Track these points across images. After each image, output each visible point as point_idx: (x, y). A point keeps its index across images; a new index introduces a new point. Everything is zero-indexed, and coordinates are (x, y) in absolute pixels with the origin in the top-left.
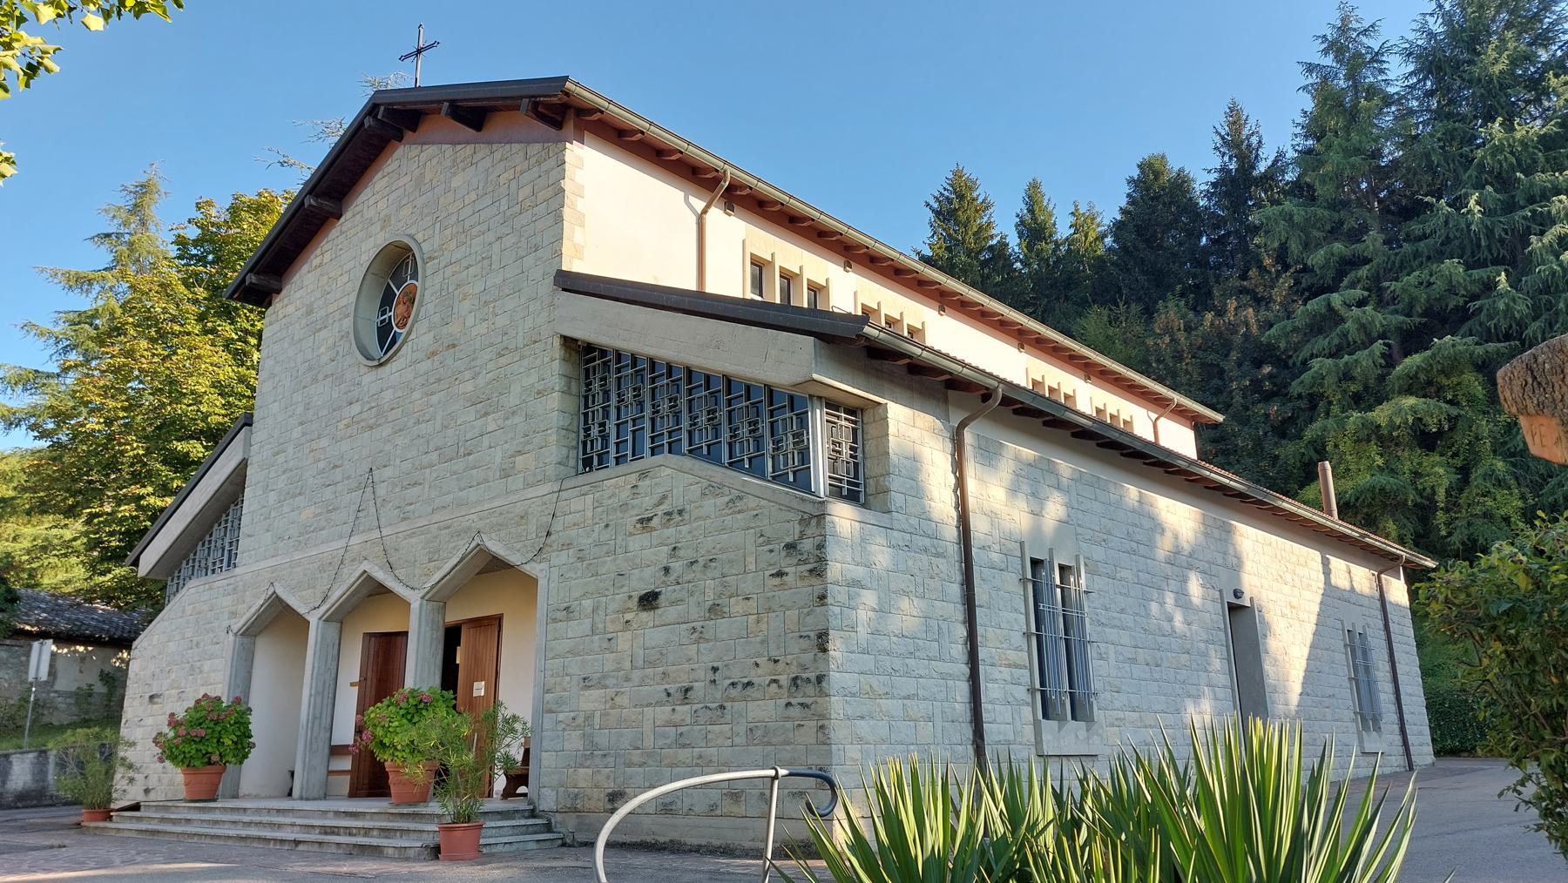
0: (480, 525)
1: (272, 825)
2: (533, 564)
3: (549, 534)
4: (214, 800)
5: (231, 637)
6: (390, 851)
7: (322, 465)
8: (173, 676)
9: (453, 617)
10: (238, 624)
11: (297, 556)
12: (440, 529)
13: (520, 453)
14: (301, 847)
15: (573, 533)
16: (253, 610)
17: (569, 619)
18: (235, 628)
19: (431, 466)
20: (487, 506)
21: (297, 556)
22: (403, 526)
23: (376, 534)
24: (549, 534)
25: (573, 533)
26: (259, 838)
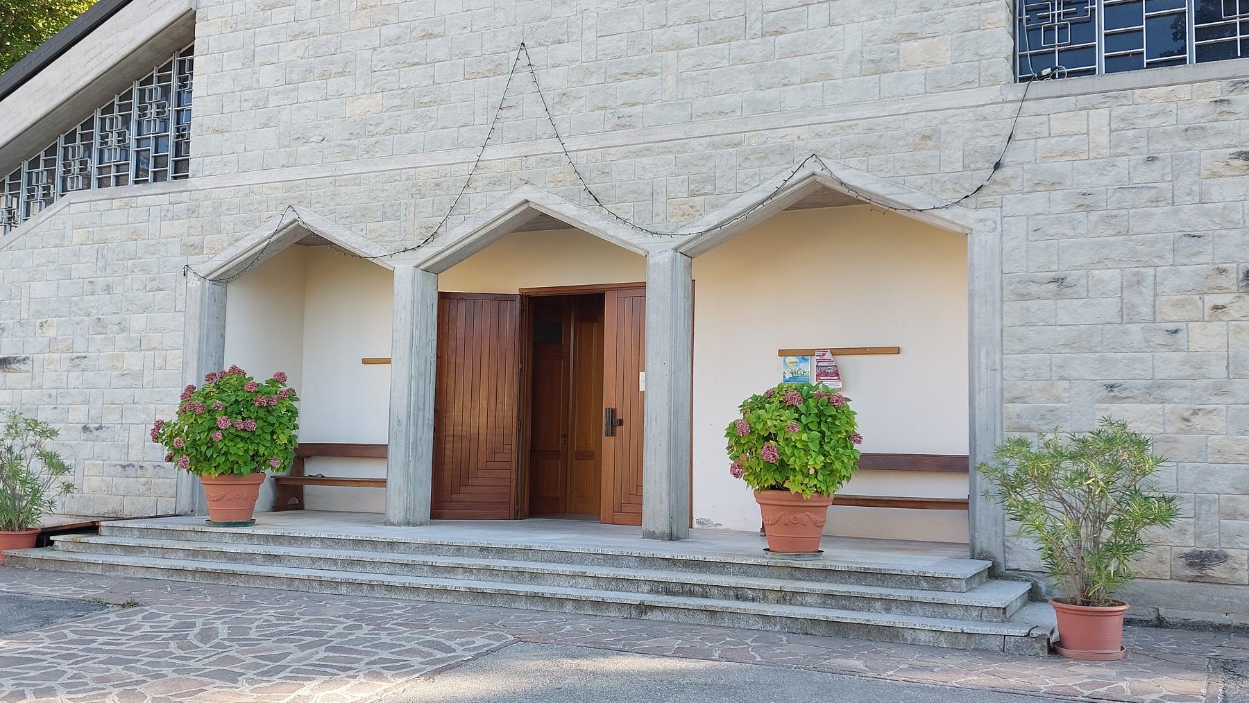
0: (819, 144)
1: (518, 575)
2: (958, 210)
3: (997, 166)
4: (250, 523)
5: (194, 282)
6: (923, 637)
7: (391, 31)
8: (52, 332)
9: (452, 283)
10: (217, 261)
11: (348, 168)
12: (715, 146)
13: (912, 36)
14: (652, 616)
15: (1062, 166)
16: (246, 244)
17: (1058, 296)
18: (204, 269)
19: (679, 46)
20: (831, 116)
21: (348, 168)
22: (618, 137)
23: (553, 146)
24: (997, 166)
25: (1062, 166)
26: (405, 588)
